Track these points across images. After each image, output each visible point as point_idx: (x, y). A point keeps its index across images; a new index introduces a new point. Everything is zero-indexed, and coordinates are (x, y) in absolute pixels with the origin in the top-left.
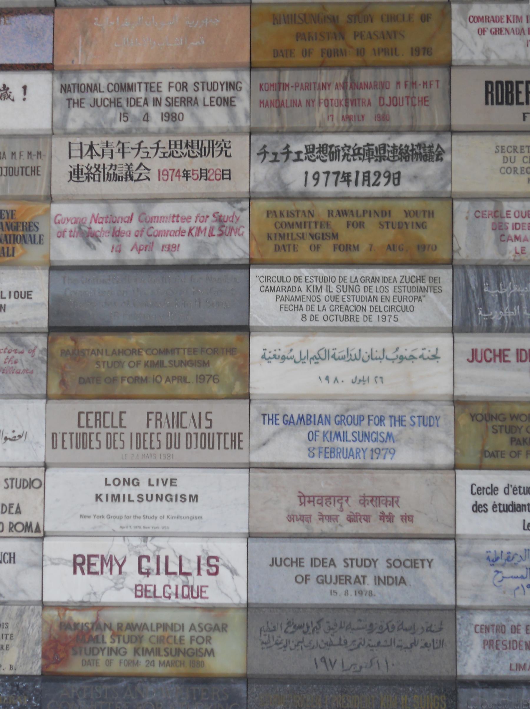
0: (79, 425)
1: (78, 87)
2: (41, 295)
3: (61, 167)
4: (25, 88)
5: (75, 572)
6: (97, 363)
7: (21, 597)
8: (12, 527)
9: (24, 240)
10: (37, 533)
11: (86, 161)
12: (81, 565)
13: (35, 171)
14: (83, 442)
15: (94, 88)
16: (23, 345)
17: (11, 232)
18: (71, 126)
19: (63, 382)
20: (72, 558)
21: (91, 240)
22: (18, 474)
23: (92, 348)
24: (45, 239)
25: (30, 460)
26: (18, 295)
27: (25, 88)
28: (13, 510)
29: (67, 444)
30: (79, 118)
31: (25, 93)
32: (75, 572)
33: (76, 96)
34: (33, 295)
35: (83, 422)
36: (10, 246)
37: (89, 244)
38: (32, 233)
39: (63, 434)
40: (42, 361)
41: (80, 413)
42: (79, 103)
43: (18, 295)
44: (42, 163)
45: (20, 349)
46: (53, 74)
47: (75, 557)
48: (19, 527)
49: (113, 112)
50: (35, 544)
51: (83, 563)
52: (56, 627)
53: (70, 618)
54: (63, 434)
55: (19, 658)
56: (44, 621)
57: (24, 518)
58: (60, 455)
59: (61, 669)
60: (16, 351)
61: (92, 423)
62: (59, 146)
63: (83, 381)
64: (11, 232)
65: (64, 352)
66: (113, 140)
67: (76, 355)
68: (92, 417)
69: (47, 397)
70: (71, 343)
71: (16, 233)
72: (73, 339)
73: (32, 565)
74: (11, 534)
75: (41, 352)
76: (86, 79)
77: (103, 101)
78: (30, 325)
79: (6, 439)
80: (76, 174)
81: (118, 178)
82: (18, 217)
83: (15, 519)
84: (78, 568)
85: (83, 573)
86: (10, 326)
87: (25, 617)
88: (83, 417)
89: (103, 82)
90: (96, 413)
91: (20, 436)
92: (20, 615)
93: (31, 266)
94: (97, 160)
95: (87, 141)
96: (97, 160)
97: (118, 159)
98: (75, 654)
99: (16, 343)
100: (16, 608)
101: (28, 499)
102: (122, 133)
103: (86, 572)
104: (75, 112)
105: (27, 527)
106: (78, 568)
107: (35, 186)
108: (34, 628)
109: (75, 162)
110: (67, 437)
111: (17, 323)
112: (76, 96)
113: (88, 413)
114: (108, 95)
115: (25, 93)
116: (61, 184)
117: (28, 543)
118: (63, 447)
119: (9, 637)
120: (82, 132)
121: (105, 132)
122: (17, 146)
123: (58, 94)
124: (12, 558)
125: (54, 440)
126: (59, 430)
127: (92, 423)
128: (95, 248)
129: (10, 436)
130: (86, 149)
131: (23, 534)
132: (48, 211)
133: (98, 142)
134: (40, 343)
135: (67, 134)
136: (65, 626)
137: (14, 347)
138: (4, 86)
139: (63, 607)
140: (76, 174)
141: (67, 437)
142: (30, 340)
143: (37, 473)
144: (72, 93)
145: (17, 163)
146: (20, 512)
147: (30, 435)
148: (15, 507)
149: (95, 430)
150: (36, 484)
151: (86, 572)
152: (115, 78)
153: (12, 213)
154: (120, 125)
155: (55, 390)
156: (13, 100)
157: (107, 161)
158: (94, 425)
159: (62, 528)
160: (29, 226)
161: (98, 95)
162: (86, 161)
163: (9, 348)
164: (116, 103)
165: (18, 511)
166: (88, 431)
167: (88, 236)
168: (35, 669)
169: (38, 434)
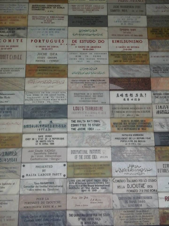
0: (164, 167)
1: (157, 94)
2: (153, 138)
3: (155, 111)
4: (145, 94)
5: (166, 201)
6: (166, 153)
7: (154, 207)
8: (151, 190)
9: (148, 126)
10: (156, 192)
11: (160, 109)
12: (167, 199)
13: (149, 112)
14: (165, 171)
15: (160, 94)
16: (150, 149)
17: (145, 125)
18: (156, 102)
19: (159, 158)
20: (164, 197)
21: (162, 126)
22: (151, 178)
23: (165, 150)
24: (152, 126)
25: (153, 175)
26: (148, 138)
27: (145, 94)
28: (151, 187)
29: (161, 171)
30: (157, 100)
31: (146, 95)
32: (166, 201)
33: (157, 96)
34: (151, 138)
35: (164, 167)
36: (145, 128)
37: (162, 127)
38: (150, 125)
39: (160, 169)
40: (154, 153)
41: (163, 164)
42: (157, 97)
43: (148, 138)
44: (151, 110)
45: (149, 150)
46: (151, 91)
47: (165, 197)
48: (152, 191)
49: (165, 99)
50: (156, 194)
51: (167, 199)
52: (162, 213)
53: (165, 211)
54: (160, 169)
55: (155, 221)
56: (159, 212)
57: (153, 188)
58: (159, 174)
59: (164, 224)
60: (148, 151)
61: (166, 167)
62: (154, 106)
63: (163, 157)
64: (145, 125)
65: (159, 151)
66: (165, 105)
67: (161, 151)
68: (166, 165)
69: (156, 161)
70: (160, 149)
71: (146, 125)
72: (160, 148)
73: (156, 199)
74: (151, 192)
75: (154, 151)
76: (159, 92)
77: (162, 97)
78: (151, 145)
79: (148, 170)
80: (158, 112)
81: (167, 113)
82: (146, 122)
83: (151, 189)
84: (166, 199)
85: (167, 201)
86: (147, 145)
87: (155, 211)
88: (164, 165)
89: (162, 93)
90: (167, 164)
91: (151, 170)
92: (154, 211)
93: (149, 132)
94: (162, 109)
95: (160, 105)
96: (162, 109)
97: (167, 109)
98: (167, 220)
99: (148, 149)
100: (153, 209)
101: (154, 184)
102: (166, 104)
103: (168, 200)
104: (157, 99)
105: (154, 190)
106: (166, 199)
107: (150, 115)
108: (157, 214)
109: (158, 110)
110: (161, 170)
111: (148, 145)
112: (157, 96)
113: (165, 164)
114: (163, 96)
115: (146, 95)
116: (155, 114)
117: (154, 194)
118: (160, 172)
119: (152, 216)
120: (158, 104)
121: (163, 103)
122: (145, 106)
123: (153, 95)
124: (151, 198)
125: (158, 171)
126: (159, 168)
127: (166, 167)
128: (163, 128)
129: (149, 170)
130: (160, 107)
131: (153, 192)
132: (153, 120)
133: (162, 105)
134: (153, 149)
135: (155, 104)
136: (165, 213)
137: (148, 150)
138: (141, 94)
139: (163, 209)
140: (158, 112)
141: (161, 170)
142: (151, 148)
143: (155, 178)
144: (156, 96)
145: (145, 110)
146: (152, 187)
147: (153, 170)
148: (151, 186)
149: (166, 168)
150: (155, 181)
151: (168, 200)
152: (165, 92)
153: (145, 121)
154: (167, 102)
155: (157, 159)
156: (143, 97)
157: (164, 109)
158: (167, 167)
159: (162, 191)
160: (149, 123)
161: (161, 96)
162: (160, 109)
163: (147, 150)
164: (165, 97)
165: (152, 187)
166: (165, 168)
167: (162, 126)
168: (159, 224)
169: (155, 169)
